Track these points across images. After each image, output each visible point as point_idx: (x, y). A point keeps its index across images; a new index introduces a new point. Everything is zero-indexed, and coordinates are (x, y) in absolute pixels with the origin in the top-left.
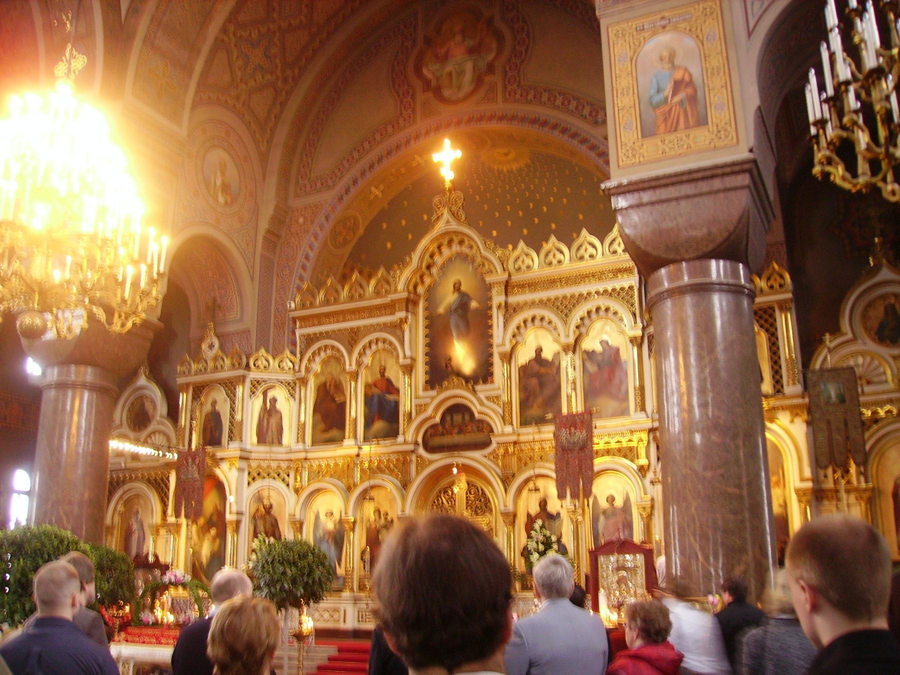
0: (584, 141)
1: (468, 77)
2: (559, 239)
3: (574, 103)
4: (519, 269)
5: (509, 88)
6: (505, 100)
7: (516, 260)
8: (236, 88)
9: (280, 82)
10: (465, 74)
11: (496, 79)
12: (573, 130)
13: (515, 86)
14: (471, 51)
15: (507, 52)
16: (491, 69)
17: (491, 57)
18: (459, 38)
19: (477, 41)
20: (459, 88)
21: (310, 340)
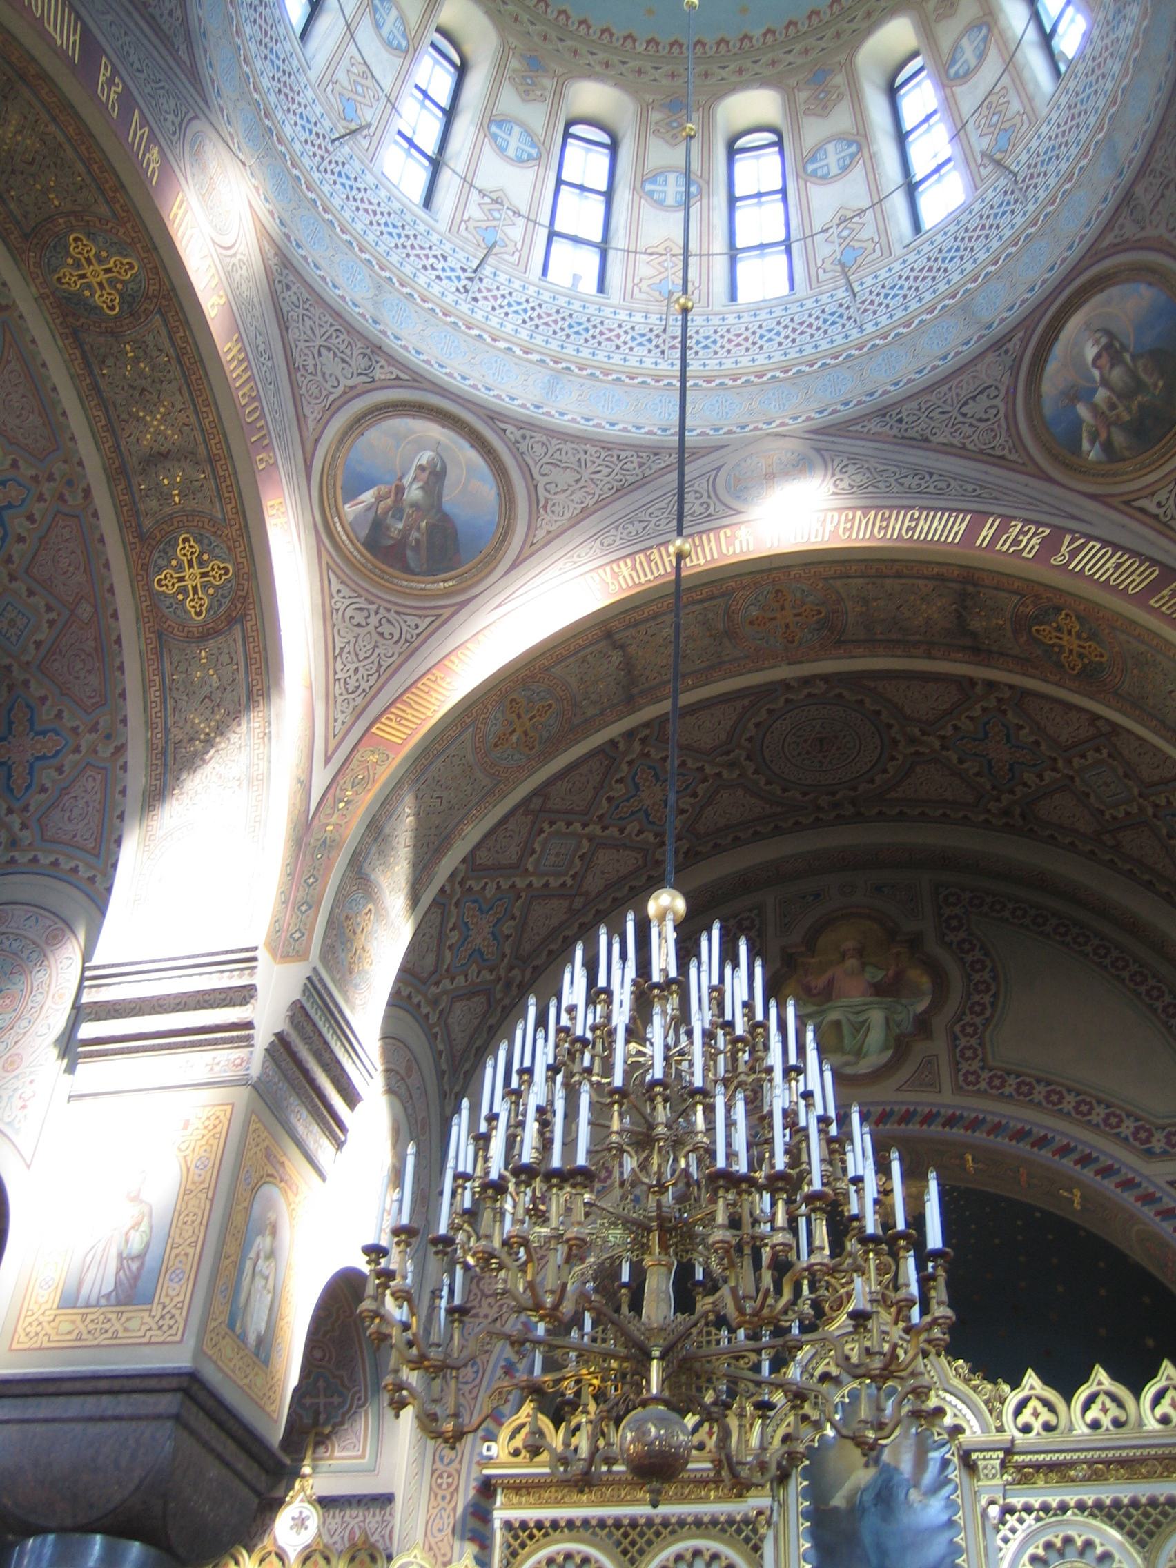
0: (1127, 1184)
1: (876, 1036)
2: (1115, 1376)
3: (1101, 1111)
4: (1026, 1429)
5: (965, 1066)
6: (958, 1089)
7: (1018, 1411)
8: (437, 984)
9: (498, 987)
10: (868, 1030)
11: (939, 1046)
12: (1105, 1161)
13: (976, 1065)
14: (879, 990)
15: (953, 1004)
16: (923, 1026)
17: (921, 1007)
18: (852, 963)
19: (891, 973)
20: (859, 1053)
21: (523, 1534)
